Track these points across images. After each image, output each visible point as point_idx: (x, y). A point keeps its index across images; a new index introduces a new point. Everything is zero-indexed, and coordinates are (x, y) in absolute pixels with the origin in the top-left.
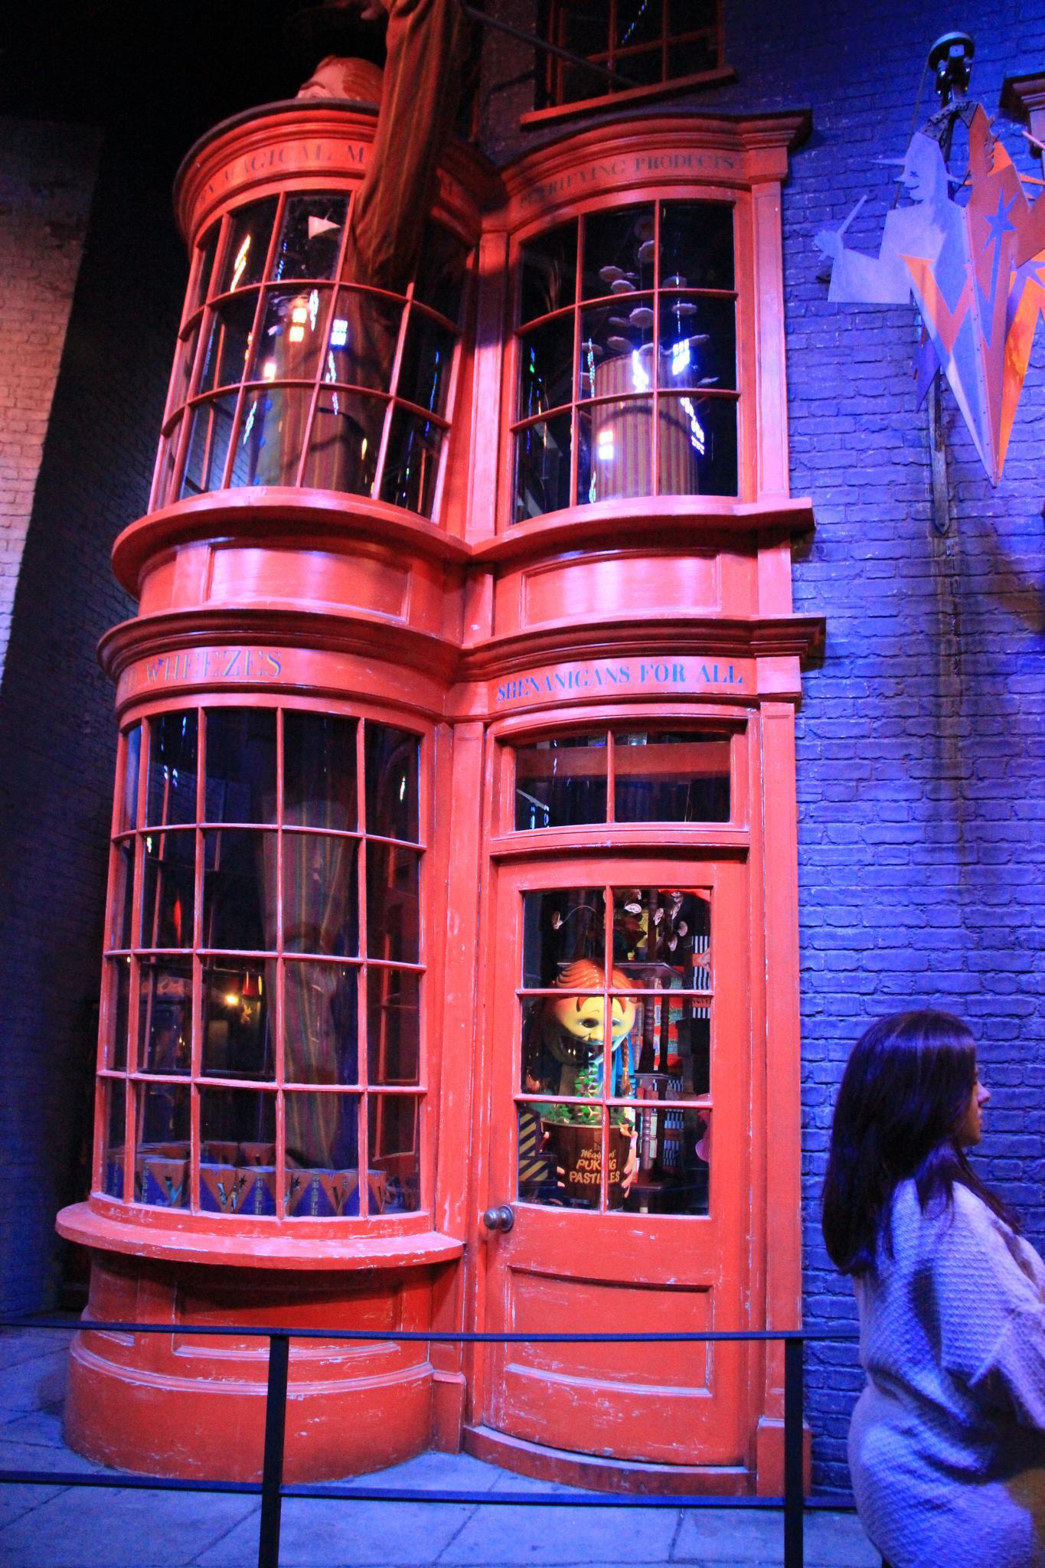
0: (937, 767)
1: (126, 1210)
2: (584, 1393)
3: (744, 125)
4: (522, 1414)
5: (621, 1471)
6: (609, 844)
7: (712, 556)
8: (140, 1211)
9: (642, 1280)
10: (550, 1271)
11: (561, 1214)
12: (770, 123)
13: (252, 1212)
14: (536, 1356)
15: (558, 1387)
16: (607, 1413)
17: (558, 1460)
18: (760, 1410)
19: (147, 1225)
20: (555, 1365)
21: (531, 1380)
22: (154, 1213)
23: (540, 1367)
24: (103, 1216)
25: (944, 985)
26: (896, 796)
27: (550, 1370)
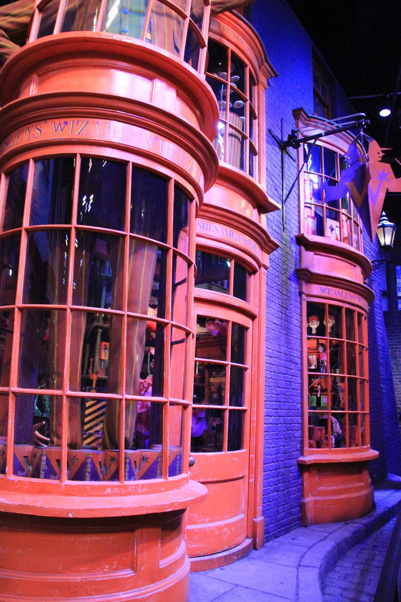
0: (282, 303)
1: (126, 487)
2: (220, 528)
3: (266, 64)
4: (195, 546)
5: (234, 554)
6: (237, 305)
7: (254, 208)
8: (138, 485)
9: (236, 477)
10: (209, 480)
11: (214, 456)
12: (269, 69)
13: (83, 479)
14: (200, 518)
15: (211, 529)
16: (226, 533)
17: (218, 558)
18: (255, 517)
19: (143, 493)
20: (207, 520)
21: (199, 529)
22: (148, 484)
23: (201, 523)
24: (101, 496)
25: (282, 371)
26: (276, 309)
27: (206, 523)
